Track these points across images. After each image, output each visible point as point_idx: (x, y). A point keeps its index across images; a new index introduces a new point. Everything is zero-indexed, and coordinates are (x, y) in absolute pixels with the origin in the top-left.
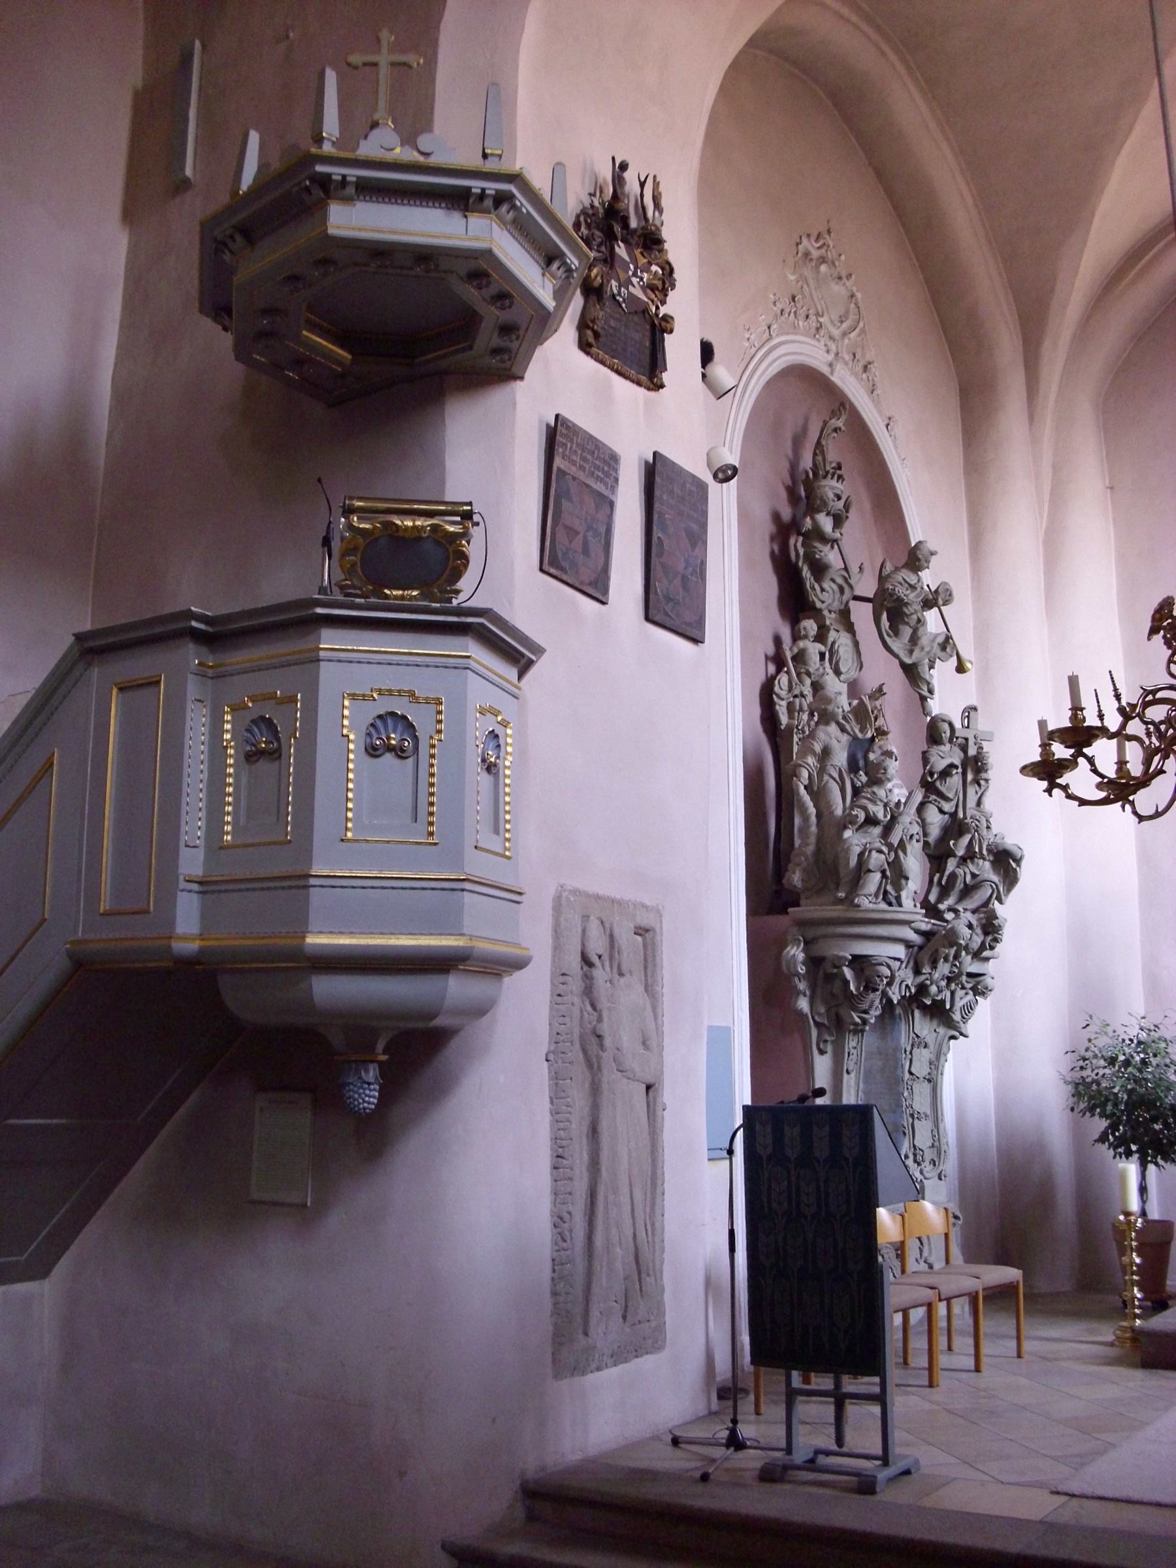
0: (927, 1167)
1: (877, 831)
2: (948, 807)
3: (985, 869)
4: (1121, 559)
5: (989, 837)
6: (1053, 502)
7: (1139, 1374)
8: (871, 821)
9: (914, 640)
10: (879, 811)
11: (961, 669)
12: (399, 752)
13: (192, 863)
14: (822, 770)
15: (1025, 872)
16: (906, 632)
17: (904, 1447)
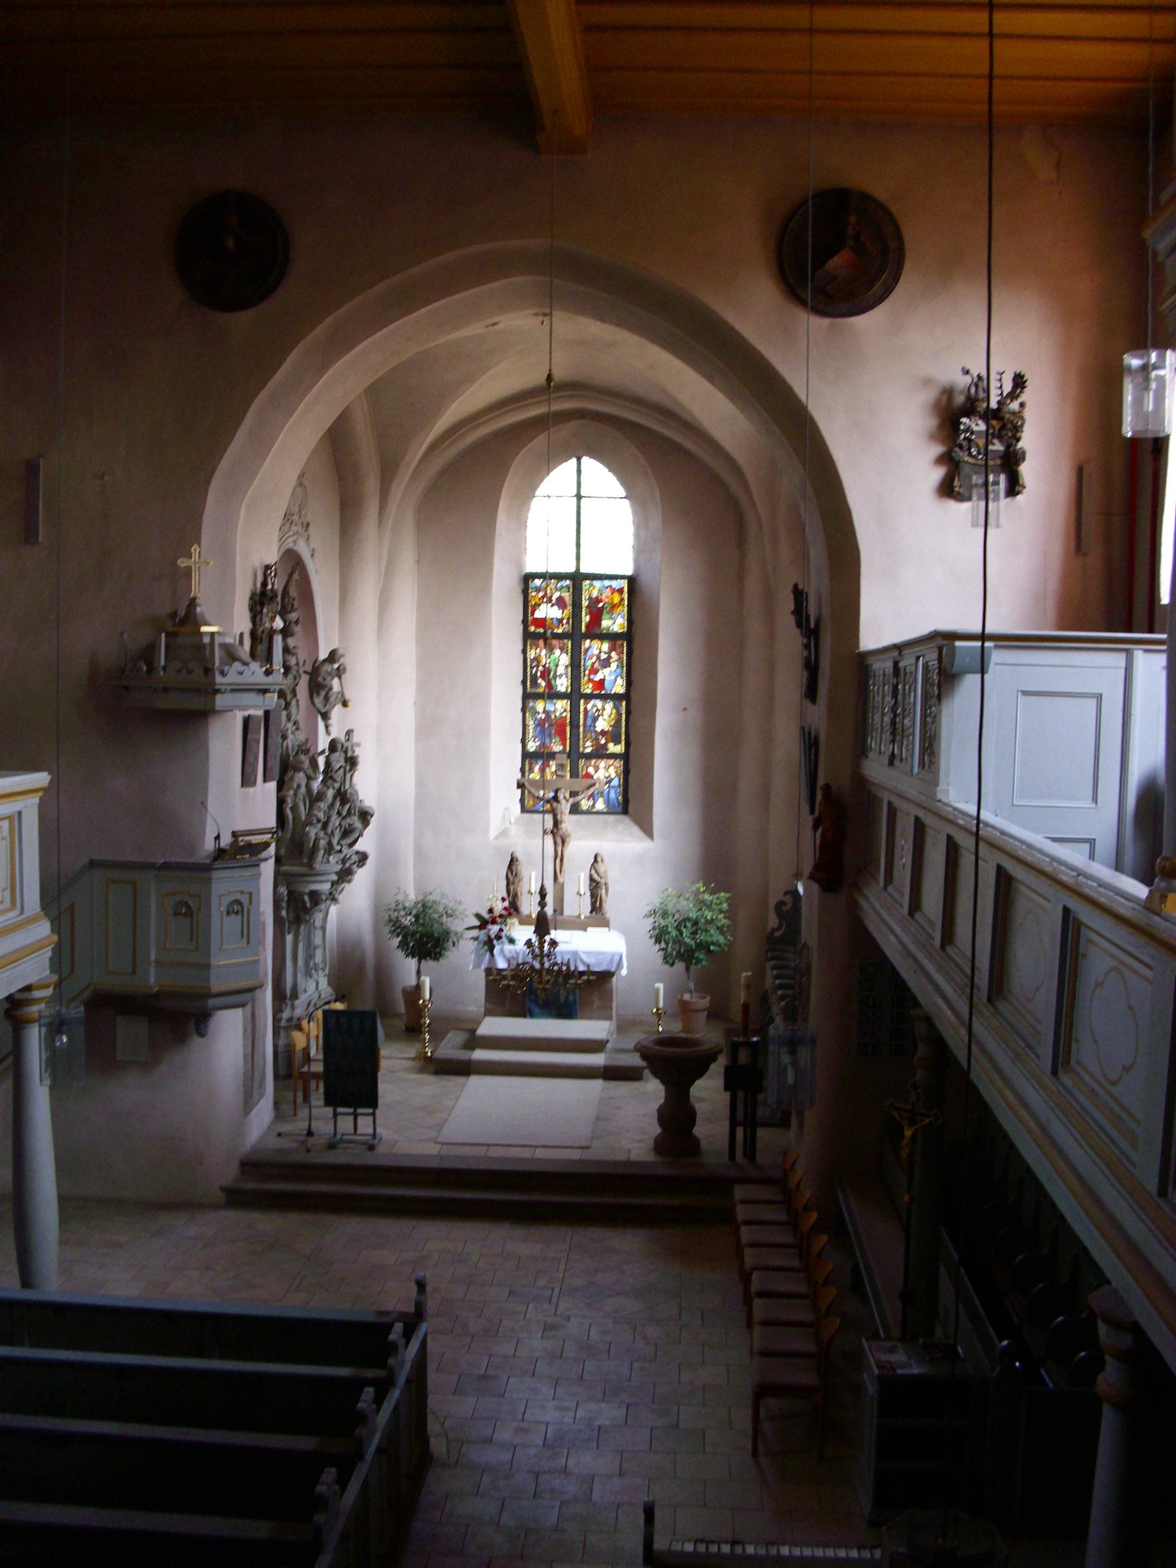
0: (320, 972)
1: (320, 825)
2: (337, 785)
3: (355, 821)
4: (420, 605)
5: (358, 804)
6: (387, 573)
7: (432, 1079)
8: (319, 821)
9: (327, 698)
10: (321, 815)
11: (345, 704)
12: (237, 913)
13: (153, 956)
14: (295, 794)
15: (373, 821)
16: (323, 693)
17: (378, 1130)
